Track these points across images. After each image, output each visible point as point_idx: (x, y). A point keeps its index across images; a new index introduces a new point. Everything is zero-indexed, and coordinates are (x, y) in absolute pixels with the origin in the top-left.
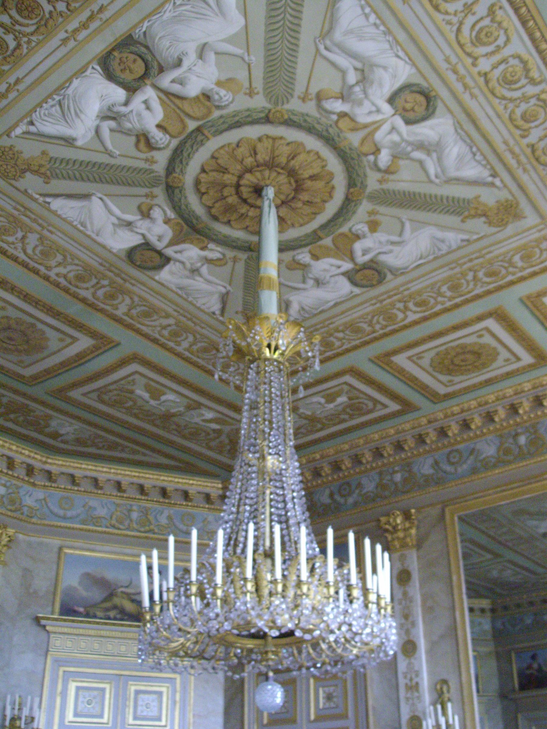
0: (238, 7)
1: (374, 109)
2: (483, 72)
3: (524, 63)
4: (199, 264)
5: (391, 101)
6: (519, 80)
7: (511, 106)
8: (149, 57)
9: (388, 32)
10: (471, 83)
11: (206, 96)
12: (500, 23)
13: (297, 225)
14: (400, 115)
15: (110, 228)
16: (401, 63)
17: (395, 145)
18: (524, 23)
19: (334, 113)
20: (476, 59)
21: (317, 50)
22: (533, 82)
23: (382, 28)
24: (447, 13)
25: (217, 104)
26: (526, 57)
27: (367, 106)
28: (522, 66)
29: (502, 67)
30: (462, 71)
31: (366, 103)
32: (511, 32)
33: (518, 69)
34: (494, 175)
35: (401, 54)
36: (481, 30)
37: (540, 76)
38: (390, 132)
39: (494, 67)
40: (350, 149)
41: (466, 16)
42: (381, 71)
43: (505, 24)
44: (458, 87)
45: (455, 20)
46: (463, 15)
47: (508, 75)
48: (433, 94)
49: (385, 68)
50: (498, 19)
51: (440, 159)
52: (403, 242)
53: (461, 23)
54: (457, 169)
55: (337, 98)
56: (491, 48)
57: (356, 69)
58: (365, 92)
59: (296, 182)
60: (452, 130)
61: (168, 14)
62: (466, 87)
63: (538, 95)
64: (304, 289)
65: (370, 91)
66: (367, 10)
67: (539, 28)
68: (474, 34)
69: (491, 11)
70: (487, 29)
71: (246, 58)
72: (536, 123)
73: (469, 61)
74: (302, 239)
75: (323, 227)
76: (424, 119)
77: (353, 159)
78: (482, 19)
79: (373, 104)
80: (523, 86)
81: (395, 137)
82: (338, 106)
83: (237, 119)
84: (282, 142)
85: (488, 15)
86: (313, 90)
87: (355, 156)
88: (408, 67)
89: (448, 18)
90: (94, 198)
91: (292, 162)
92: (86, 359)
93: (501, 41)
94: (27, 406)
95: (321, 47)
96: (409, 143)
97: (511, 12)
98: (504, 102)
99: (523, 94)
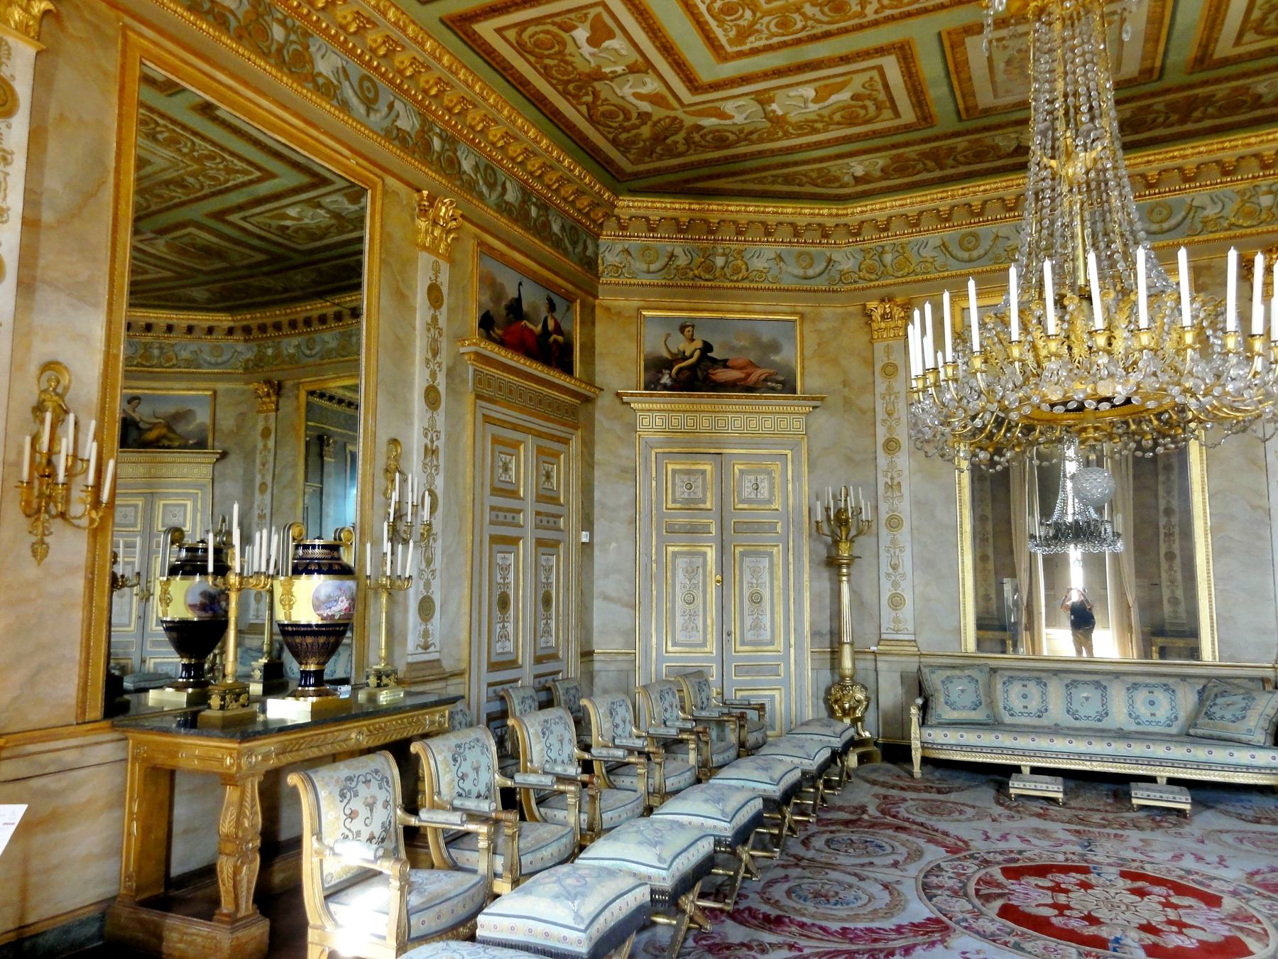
92: (1168, 13)
94: (1196, 96)
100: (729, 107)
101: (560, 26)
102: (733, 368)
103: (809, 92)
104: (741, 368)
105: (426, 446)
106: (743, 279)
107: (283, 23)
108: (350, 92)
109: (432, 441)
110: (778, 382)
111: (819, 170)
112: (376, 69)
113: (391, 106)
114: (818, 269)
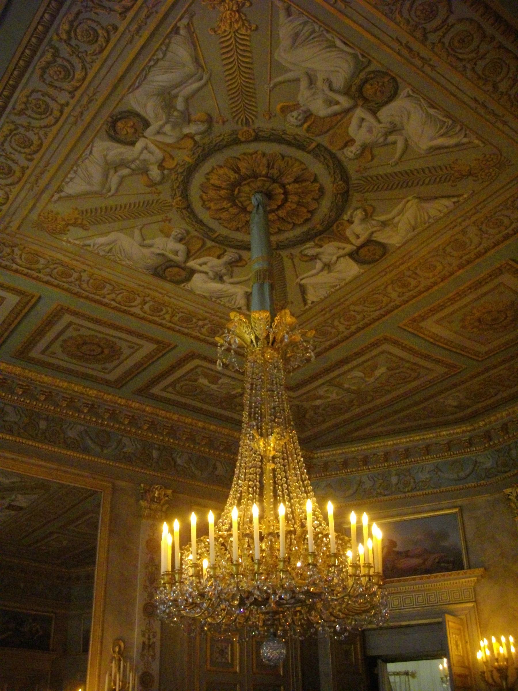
0: (107, 236)
1: (145, 151)
2: (70, 95)
3: (44, 70)
4: (374, 222)
5: (133, 144)
6: (60, 65)
7: (88, 59)
8: (164, 267)
9: (76, 164)
10: (85, 100)
11: (181, 240)
12: (25, 103)
13: (303, 167)
14: (142, 133)
15: (332, 274)
16: (95, 150)
17: (175, 126)
18: (14, 88)
19: (163, 173)
20: (62, 106)
21: (113, 195)
22: (56, 53)
23: (75, 168)
24: (40, 138)
25: (185, 234)
26: (38, 72)
27: (145, 155)
28: (47, 71)
29: (57, 84)
30: (78, 109)
31: (142, 157)
32: (26, 92)
33: (51, 72)
34: (176, 30)
35: (87, 152)
36: (37, 113)
37: (48, 51)
38: (165, 134)
39: (61, 89)
40: (194, 154)
41: (34, 127)
42: (108, 158)
43: (25, 100)
44: (95, 106)
45: (41, 133)
46: (34, 129)
47: (61, 76)
48: (110, 119)
49: (105, 156)
50: (23, 106)
51: (175, 86)
52: (308, 74)
53: (41, 127)
54: (184, 65)
55: (147, 175)
56: (47, 99)
57: (116, 171)
58: (133, 161)
59: (233, 191)
60: (141, 89)
61: (128, 262)
62: (90, 101)
63: (65, 42)
64: (406, 140)
65: (130, 158)
66: (67, 180)
67: (11, 75)
68: (43, 116)
69: (21, 113)
70: (35, 108)
71: (140, 227)
72: (94, 25)
73: (67, 110)
74: (322, 159)
75: (301, 147)
76: (138, 115)
77: (203, 150)
78: (29, 116)
79: (141, 153)
80: (64, 59)
81: (168, 128)
82: (155, 173)
83: (194, 223)
84: (204, 197)
85: (24, 113)
86: (149, 190)
87: (200, 150)
88: (95, 144)
89: (43, 137)
90: (303, 282)
91: (223, 186)
93: (39, 95)
95: (109, 194)
96: (169, 115)
97: (13, 101)
98: (88, 66)
99: (71, 55)
100: (321, 392)
101: (190, 380)
102: (412, 557)
103: (357, 373)
104: (419, 556)
105: (144, 643)
106: (412, 490)
107: (47, 419)
108: (90, 442)
109: (149, 639)
110: (448, 562)
111: (424, 408)
112: (107, 425)
113: (120, 441)
114: (468, 471)
